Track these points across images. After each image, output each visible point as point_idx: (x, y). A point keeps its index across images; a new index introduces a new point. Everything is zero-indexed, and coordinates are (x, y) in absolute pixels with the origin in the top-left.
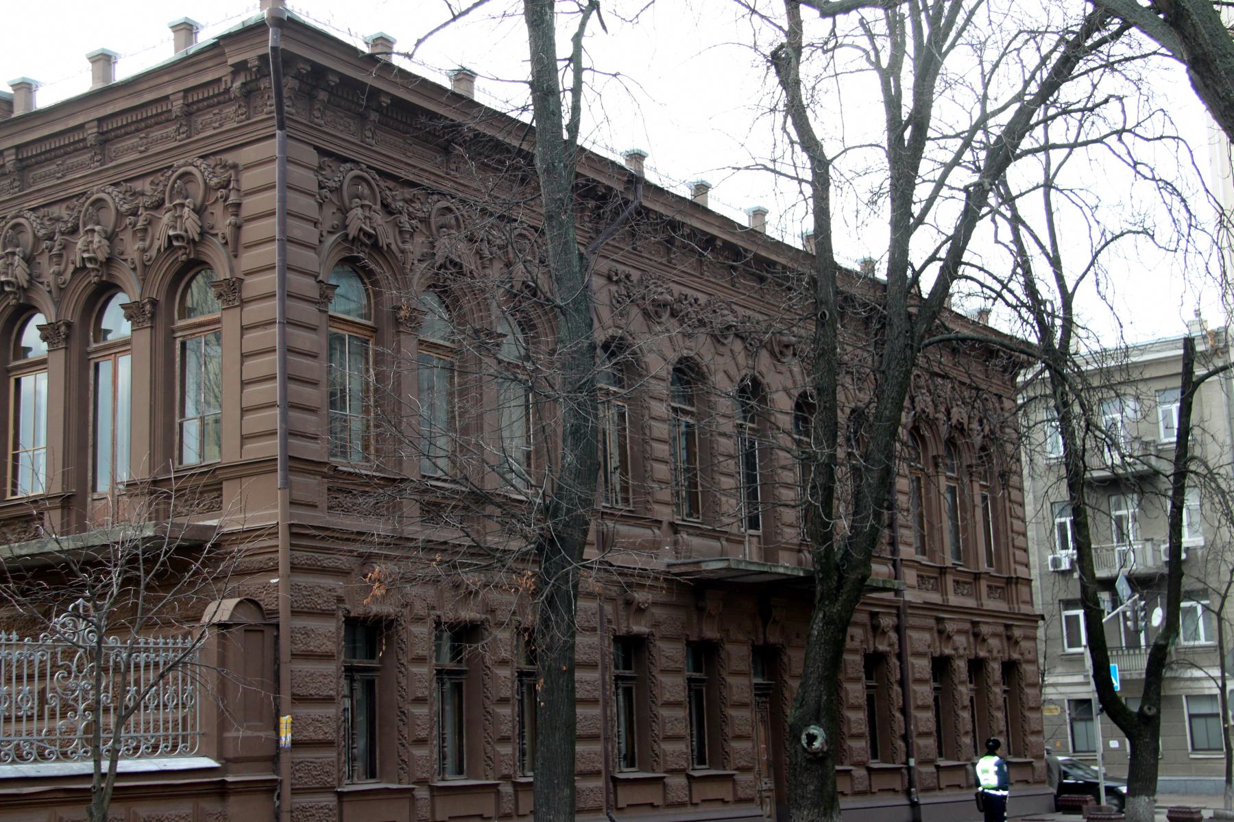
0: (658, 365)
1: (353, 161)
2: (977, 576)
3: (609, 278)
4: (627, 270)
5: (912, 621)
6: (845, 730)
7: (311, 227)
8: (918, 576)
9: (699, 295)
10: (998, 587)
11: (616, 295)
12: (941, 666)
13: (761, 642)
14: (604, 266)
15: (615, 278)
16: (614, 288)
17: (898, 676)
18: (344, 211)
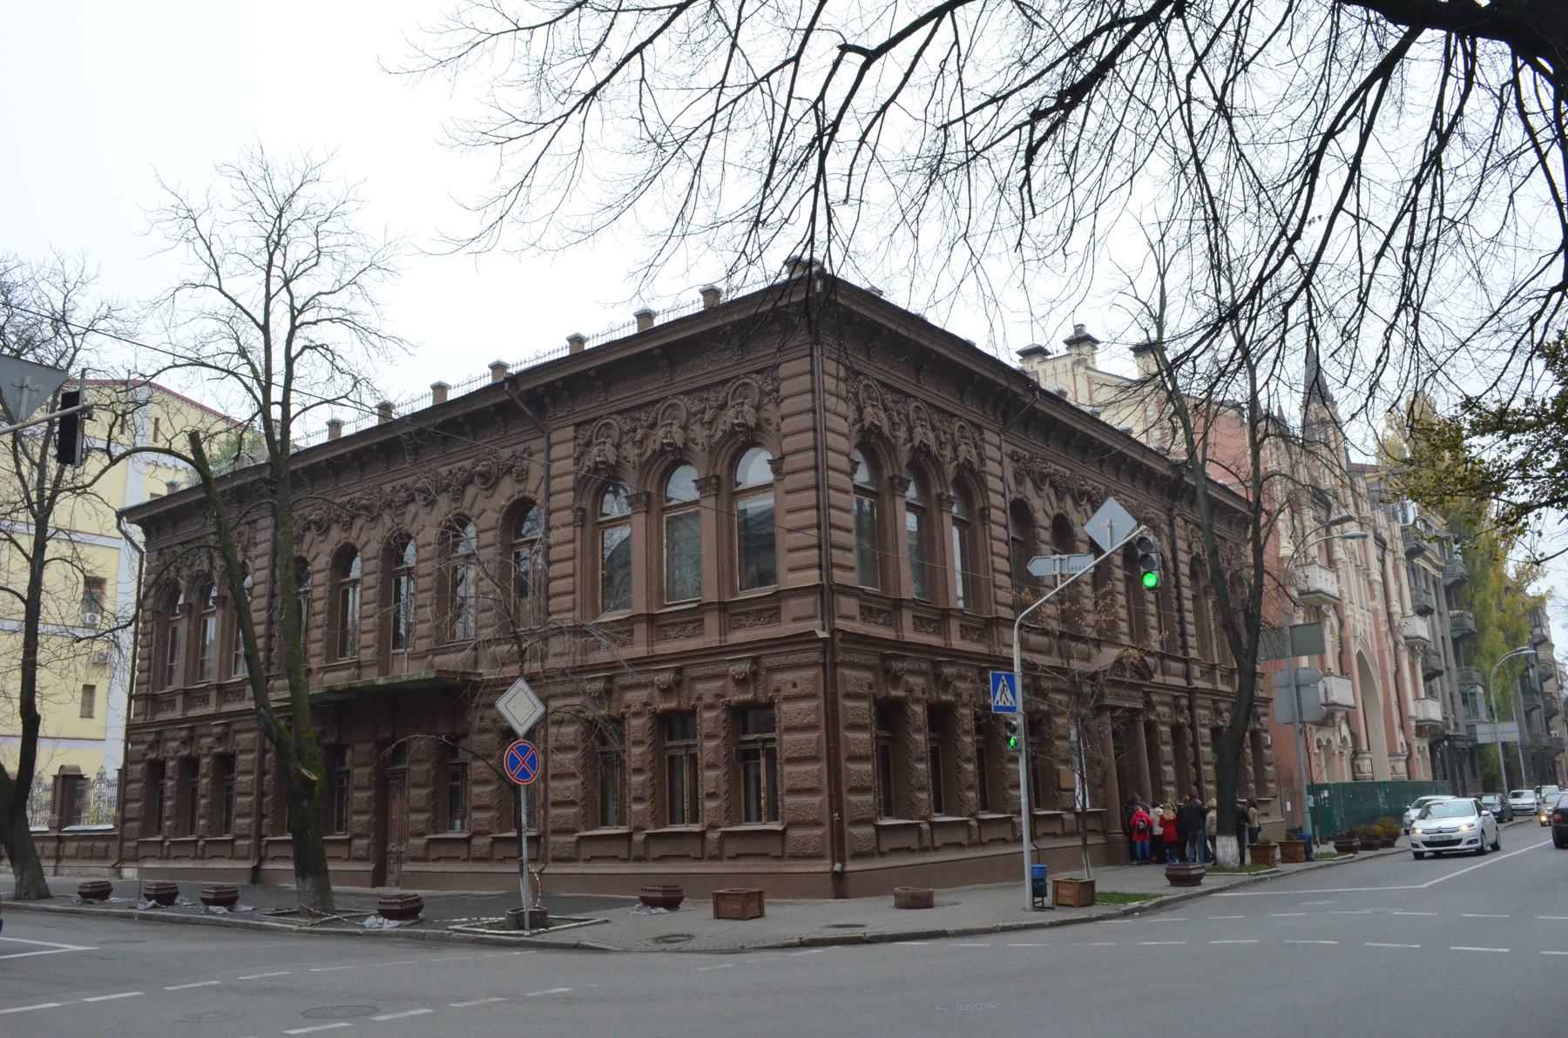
0: (1043, 520)
2: (1213, 667)
3: (1012, 458)
7: (843, 421)
18: (860, 410)
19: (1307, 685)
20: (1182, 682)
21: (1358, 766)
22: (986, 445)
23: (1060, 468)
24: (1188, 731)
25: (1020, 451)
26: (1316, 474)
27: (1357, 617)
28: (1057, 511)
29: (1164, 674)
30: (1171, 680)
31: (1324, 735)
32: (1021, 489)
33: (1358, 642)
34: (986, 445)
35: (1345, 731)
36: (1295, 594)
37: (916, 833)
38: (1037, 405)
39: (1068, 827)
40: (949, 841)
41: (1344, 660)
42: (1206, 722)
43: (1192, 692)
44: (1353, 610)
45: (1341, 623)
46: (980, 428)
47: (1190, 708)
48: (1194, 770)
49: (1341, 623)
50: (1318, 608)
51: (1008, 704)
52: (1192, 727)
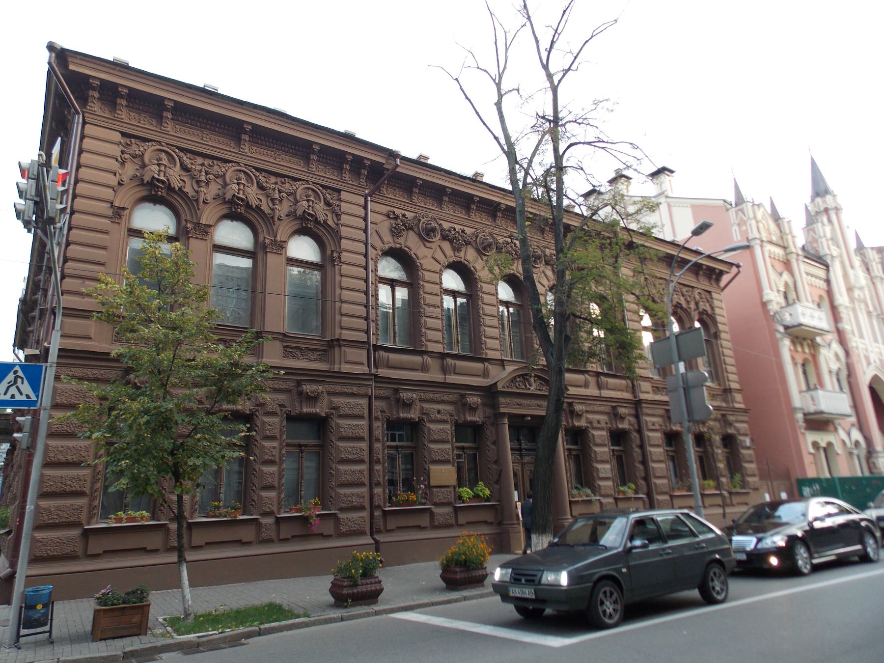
1: (155, 141)
3: (388, 216)
4: (462, 227)
5: (645, 411)
6: (595, 475)
7: (111, 176)
8: (653, 387)
9: (456, 226)
10: (718, 395)
11: (394, 225)
12: (672, 438)
13: (571, 425)
14: (385, 209)
15: (392, 216)
16: (393, 222)
17: (638, 442)
19: (694, 387)
20: (627, 395)
21: (874, 463)
22: (343, 204)
23: (458, 227)
24: (635, 435)
25: (397, 211)
26: (815, 245)
27: (869, 348)
28: (451, 260)
29: (600, 387)
30: (605, 393)
31: (823, 439)
32: (402, 240)
33: (872, 367)
34: (343, 204)
35: (856, 435)
36: (781, 329)
37: (428, 515)
38: (398, 170)
39: (439, 520)
40: (473, 520)
41: (852, 380)
42: (657, 427)
43: (637, 404)
44: (865, 344)
45: (847, 353)
46: (339, 191)
47: (637, 416)
48: (641, 467)
49: (847, 353)
50: (813, 341)
51: (18, 397)
52: (639, 431)
